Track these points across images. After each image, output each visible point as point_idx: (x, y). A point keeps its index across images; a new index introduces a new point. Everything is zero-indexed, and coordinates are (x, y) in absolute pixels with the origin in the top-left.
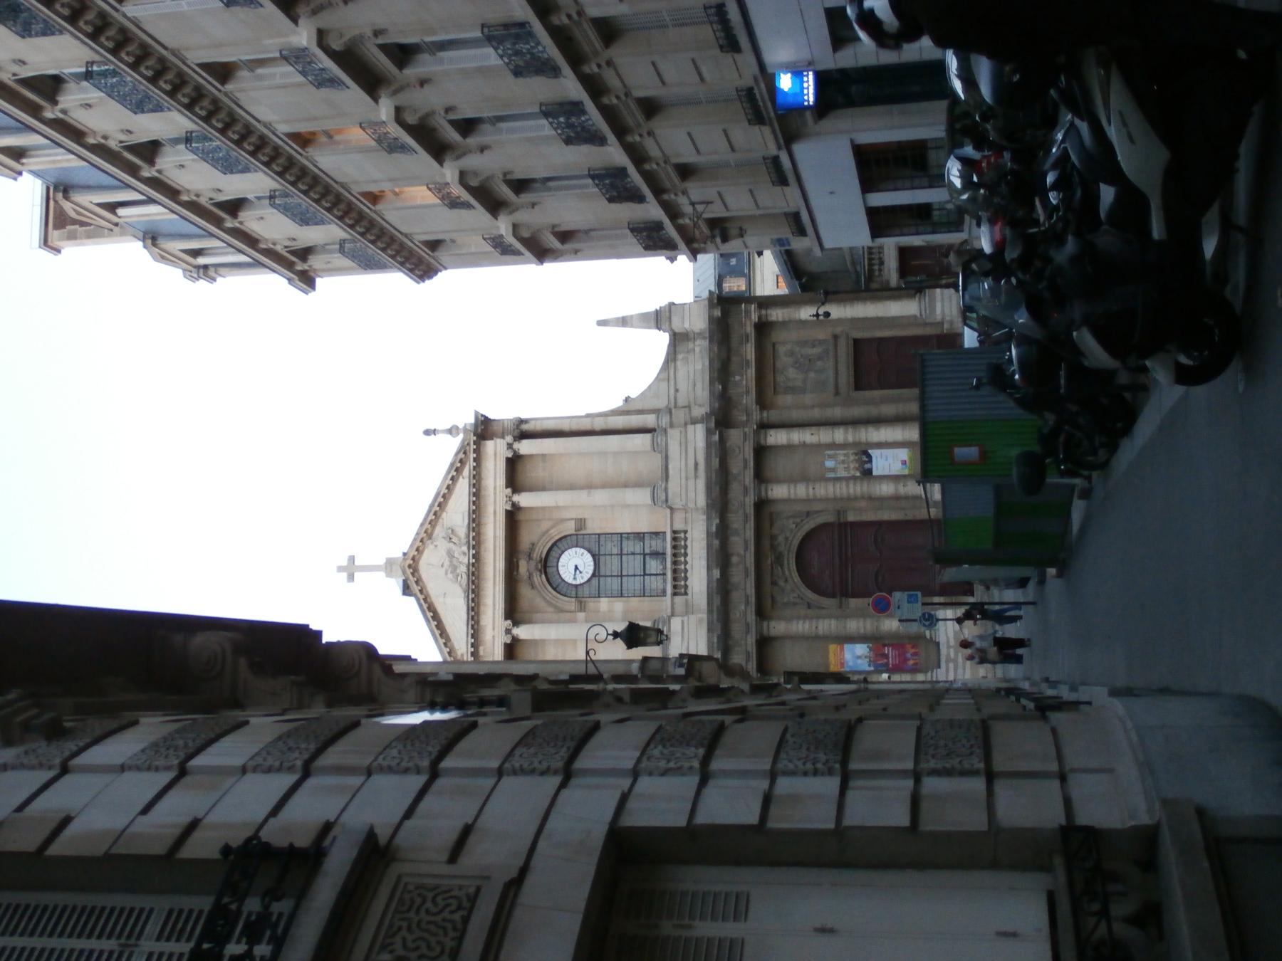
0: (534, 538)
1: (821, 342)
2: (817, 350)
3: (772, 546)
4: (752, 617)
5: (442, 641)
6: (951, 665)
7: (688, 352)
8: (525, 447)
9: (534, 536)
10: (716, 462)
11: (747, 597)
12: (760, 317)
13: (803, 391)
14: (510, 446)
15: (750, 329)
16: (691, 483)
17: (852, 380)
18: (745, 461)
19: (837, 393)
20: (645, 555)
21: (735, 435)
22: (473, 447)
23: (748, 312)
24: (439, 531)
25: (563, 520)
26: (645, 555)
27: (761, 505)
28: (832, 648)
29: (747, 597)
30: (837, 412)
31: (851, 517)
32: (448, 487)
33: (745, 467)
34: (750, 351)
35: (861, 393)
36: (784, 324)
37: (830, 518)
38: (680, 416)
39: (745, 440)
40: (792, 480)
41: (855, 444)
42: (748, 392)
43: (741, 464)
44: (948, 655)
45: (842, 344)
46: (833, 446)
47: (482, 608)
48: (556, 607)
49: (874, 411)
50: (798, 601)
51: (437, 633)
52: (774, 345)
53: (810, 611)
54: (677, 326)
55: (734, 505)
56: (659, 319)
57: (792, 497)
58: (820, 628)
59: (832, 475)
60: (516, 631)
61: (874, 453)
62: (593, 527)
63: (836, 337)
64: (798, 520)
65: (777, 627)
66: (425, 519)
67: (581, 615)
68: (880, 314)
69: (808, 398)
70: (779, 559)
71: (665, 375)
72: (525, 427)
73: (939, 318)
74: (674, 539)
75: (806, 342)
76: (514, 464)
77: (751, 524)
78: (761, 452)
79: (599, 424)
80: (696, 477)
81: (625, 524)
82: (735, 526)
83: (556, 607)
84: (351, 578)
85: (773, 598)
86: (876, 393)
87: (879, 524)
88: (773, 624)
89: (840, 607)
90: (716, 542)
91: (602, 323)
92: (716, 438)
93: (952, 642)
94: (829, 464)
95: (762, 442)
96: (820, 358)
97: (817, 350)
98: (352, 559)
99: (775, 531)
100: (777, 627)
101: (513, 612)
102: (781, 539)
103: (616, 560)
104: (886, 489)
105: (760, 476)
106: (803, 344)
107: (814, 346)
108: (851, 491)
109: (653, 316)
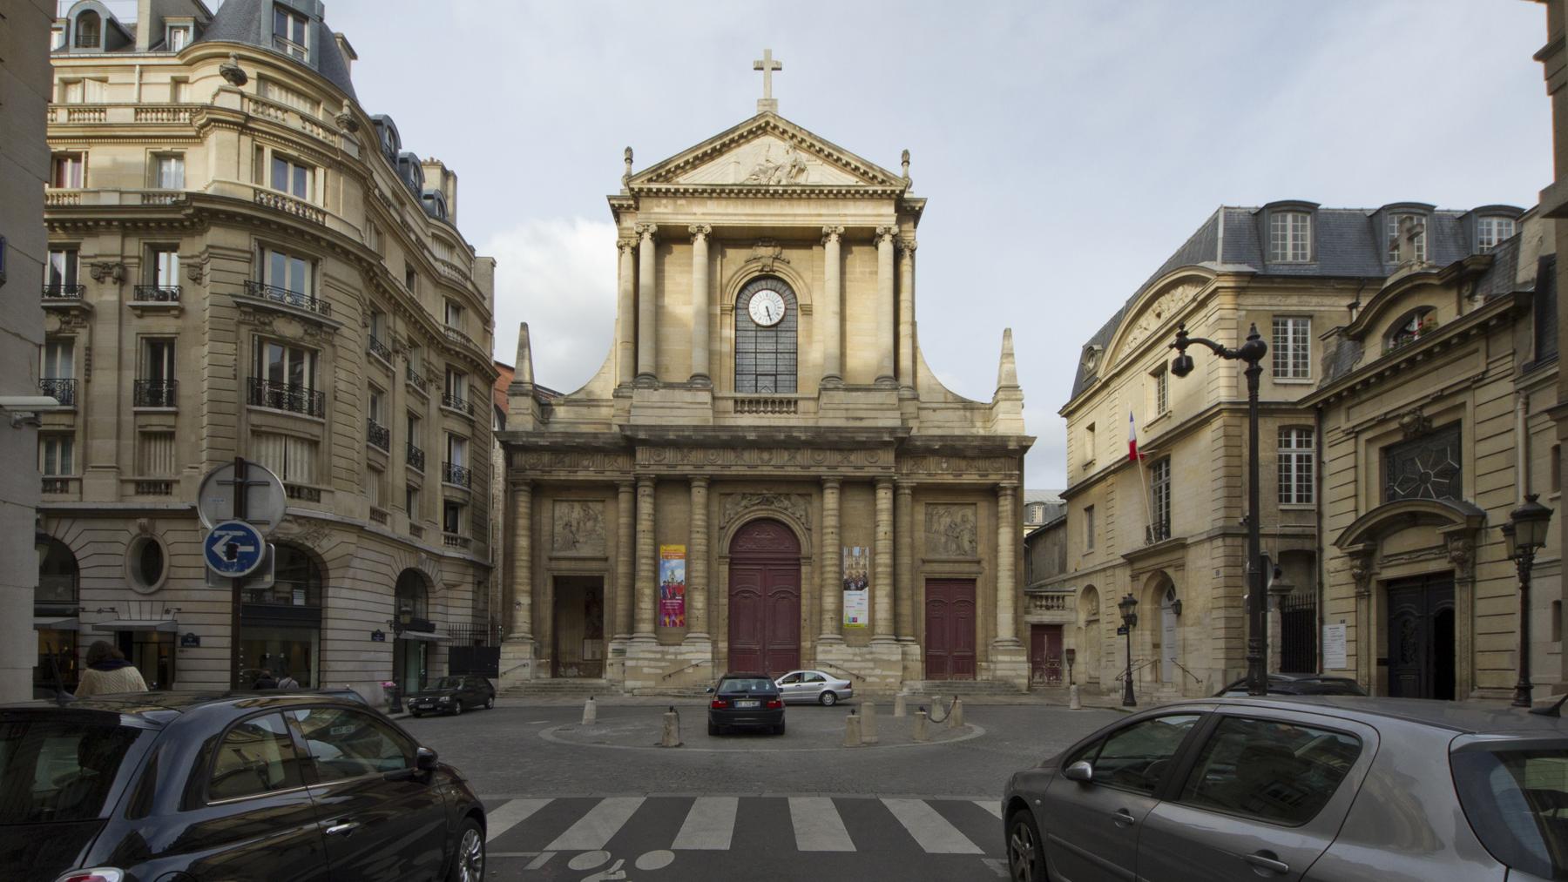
4: (709, 470)
13: (928, 530)
15: (993, 478)
17: (937, 576)
18: (862, 468)
19: (924, 562)
21: (888, 458)
23: (1011, 476)
25: (810, 293)
28: (682, 548)
30: (905, 560)
31: (804, 569)
33: (856, 468)
34: (970, 478)
35: (923, 583)
36: (996, 516)
37: (805, 550)
40: (841, 514)
41: (875, 575)
45: (974, 568)
46: (874, 553)
49: (905, 594)
54: (1002, 406)
55: (819, 456)
59: (845, 552)
61: (865, 593)
63: (979, 562)
65: (699, 494)
69: (920, 535)
70: (768, 501)
74: (789, 402)
77: (799, 472)
78: (870, 485)
82: (799, 456)
86: (922, 598)
87: (799, 597)
88: (703, 491)
90: (782, 436)
94: (856, 551)
96: (959, 547)
100: (699, 494)
103: (772, 347)
104: (829, 601)
105: (847, 485)
106: (974, 531)
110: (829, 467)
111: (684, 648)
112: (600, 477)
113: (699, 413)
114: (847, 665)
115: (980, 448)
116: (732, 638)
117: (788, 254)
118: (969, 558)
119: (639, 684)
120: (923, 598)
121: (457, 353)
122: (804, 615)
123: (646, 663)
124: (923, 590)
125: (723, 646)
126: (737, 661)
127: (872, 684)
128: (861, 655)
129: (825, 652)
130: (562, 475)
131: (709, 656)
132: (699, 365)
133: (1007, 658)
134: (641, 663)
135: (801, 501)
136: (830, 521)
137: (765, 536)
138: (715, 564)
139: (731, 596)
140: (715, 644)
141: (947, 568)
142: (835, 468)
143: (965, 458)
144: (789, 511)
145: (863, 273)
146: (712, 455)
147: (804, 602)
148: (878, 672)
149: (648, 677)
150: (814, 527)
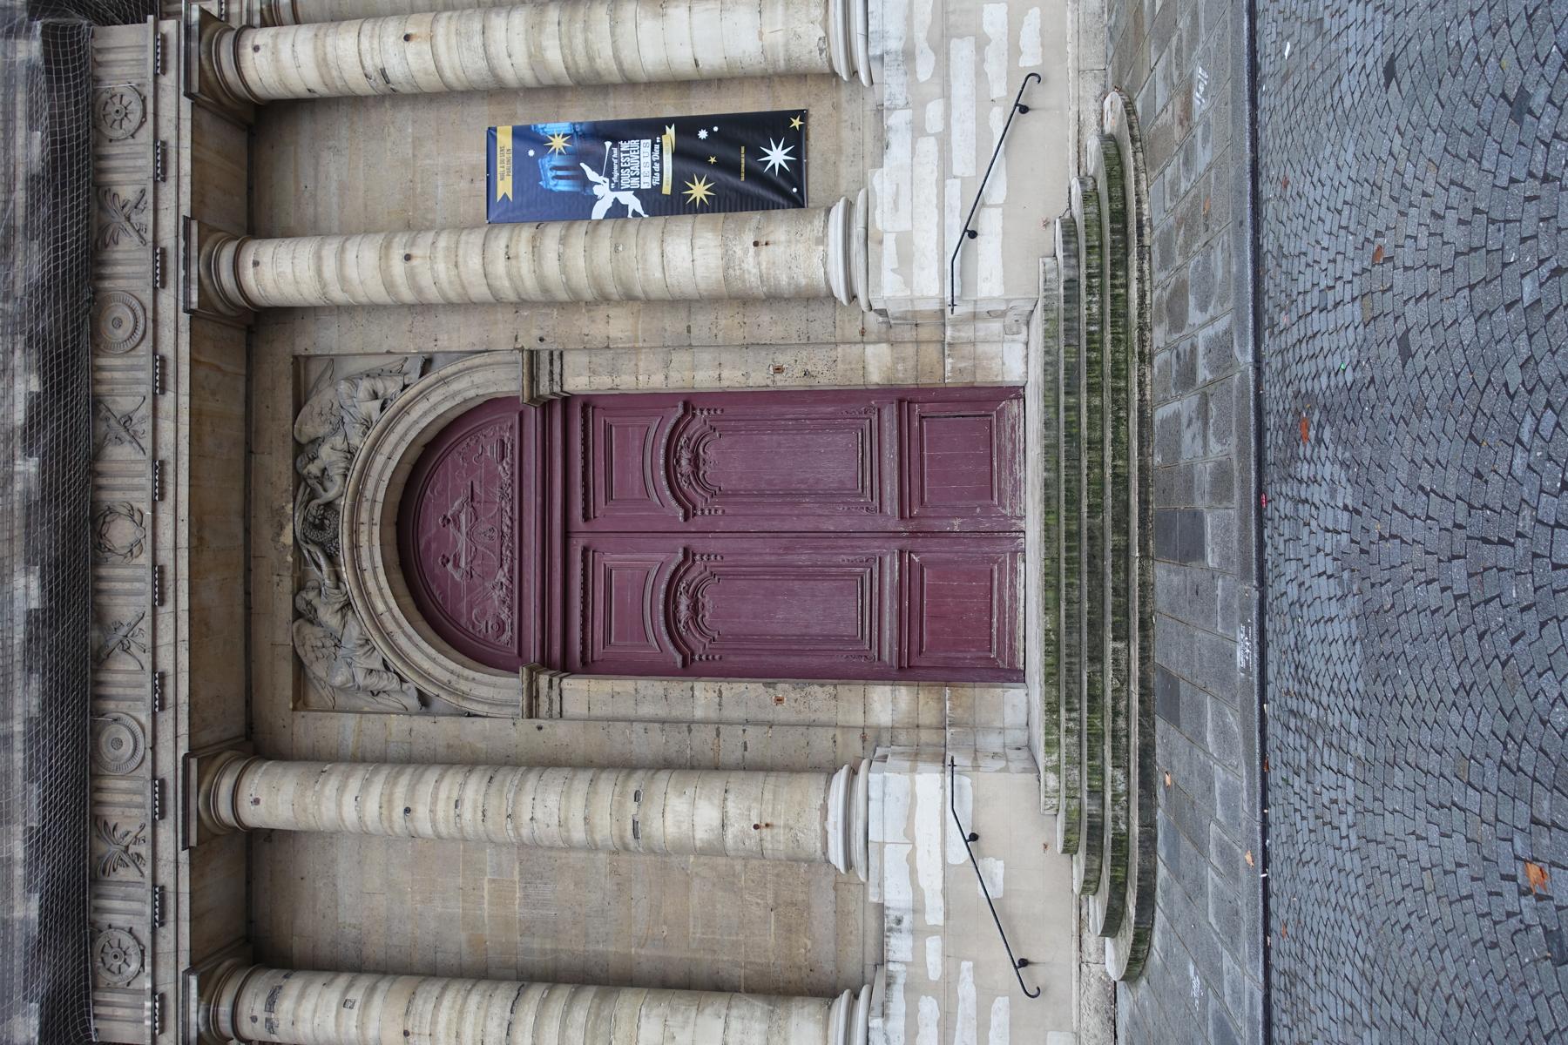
3: (299, 479)
6: (929, 1008)
11: (159, 679)
18: (161, 151)
29: (159, 679)
31: (577, 382)
33: (160, 176)
37: (505, 381)
39: (161, 68)
43: (147, 162)
50: (388, 682)
53: (422, 724)
55: (121, 323)
57: (337, 295)
58: (421, 811)
65: (270, 798)
70: (320, 524)
85: (300, 667)
87: (690, 402)
89: (532, 712)
93: (935, 917)
99: (311, 427)
100: (270, 798)
102: (328, 454)
108: (551, 267)
110: (159, 282)
111: (896, 895)
114: (965, 163)
125: (887, 704)
126: (944, 646)
128: (916, 104)
129: (906, 259)
131: (929, 781)
135: (323, 398)
138: (559, 733)
139: (689, 668)
140: (877, 743)
142: (160, 255)
144: (362, 438)
150: (406, 339)
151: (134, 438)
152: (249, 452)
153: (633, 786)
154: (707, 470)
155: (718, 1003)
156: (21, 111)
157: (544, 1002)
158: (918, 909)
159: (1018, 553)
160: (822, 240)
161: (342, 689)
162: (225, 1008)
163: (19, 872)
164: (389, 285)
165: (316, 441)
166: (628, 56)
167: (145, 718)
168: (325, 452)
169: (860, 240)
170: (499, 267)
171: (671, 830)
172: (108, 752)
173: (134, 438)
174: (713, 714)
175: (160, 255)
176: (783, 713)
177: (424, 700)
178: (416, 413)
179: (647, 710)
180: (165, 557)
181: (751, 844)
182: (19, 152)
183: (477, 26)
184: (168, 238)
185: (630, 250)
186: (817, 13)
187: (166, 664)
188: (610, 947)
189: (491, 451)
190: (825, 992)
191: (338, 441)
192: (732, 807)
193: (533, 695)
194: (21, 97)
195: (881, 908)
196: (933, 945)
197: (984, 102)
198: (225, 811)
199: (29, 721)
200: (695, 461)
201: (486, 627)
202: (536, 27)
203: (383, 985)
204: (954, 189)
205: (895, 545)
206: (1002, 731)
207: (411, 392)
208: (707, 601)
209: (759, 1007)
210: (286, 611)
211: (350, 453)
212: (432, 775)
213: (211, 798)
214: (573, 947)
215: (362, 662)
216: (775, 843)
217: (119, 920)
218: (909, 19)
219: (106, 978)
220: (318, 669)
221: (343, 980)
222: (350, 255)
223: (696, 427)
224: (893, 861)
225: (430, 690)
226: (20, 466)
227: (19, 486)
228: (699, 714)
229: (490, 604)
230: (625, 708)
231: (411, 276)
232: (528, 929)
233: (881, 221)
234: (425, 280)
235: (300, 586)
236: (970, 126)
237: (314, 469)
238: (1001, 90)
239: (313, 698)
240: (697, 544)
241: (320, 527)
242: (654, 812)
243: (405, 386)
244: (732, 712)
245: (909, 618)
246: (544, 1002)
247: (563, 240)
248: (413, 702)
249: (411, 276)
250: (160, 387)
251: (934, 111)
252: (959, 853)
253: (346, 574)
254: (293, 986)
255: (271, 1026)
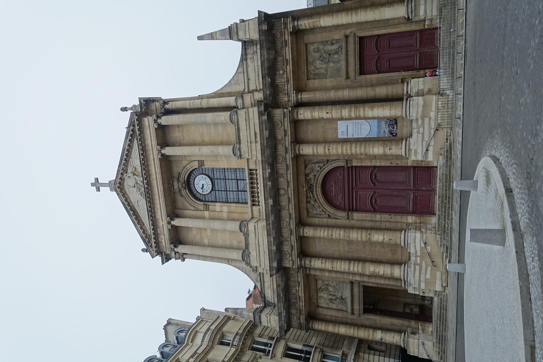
0: (180, 170)
1: (338, 41)
2: (335, 47)
3: (306, 180)
4: (293, 226)
5: (139, 226)
6: (417, 267)
7: (253, 54)
8: (165, 120)
9: (181, 169)
10: (266, 133)
11: (290, 215)
12: (294, 27)
14: (156, 121)
15: (288, 37)
16: (253, 145)
17: (358, 67)
19: (348, 77)
20: (237, 180)
21: (278, 113)
22: (136, 123)
23: (285, 24)
24: (130, 170)
26: (237, 180)
27: (297, 157)
29: (290, 215)
30: (346, 94)
31: (355, 164)
32: (129, 145)
33: (285, 135)
34: (288, 53)
35: (363, 77)
36: (312, 30)
38: (248, 99)
39: (284, 117)
40: (316, 142)
42: (288, 81)
44: (416, 260)
45: (351, 40)
47: (156, 209)
48: (194, 207)
49: (370, 93)
51: (136, 222)
52: (306, 44)
53: (329, 220)
54: (241, 36)
55: (280, 159)
56: (231, 33)
58: (334, 235)
60: (173, 223)
62: (208, 165)
63: (347, 37)
64: (322, 165)
65: (309, 232)
66: (120, 163)
67: (207, 213)
68: (377, 18)
69: (329, 82)
70: (310, 188)
71: (241, 70)
72: (167, 106)
73: (422, 18)
74: (251, 174)
75: (327, 42)
76: (162, 131)
77: (290, 171)
78: (296, 123)
79: (205, 103)
80: (256, 142)
81: (223, 164)
82: (281, 172)
83: (194, 207)
84: (98, 190)
89: (348, 219)
91: (200, 38)
92: (265, 117)
93: (419, 254)
95: (296, 118)
96: (336, 53)
97: (335, 47)
98: (97, 179)
99: (308, 171)
101: (173, 213)
103: (223, 182)
107: (332, 44)
108: (353, 151)
109: (228, 33)
110: (286, 152)
111: (412, 251)
112: (302, 284)
113: (260, 230)
114: (426, 138)
115: (269, 49)
116: (405, 212)
117: (176, 174)
118: (344, 45)
119: (438, 282)
120: (375, 76)
121: (243, 344)
122: (388, 164)
123: (423, 276)
124: (368, 76)
125: (411, 219)
127: (443, 119)
128: (418, 128)
130: (302, 304)
132: (235, 226)
133: (422, 8)
134: (423, 279)
135: (310, 166)
136: (321, 150)
137: (333, 189)
138: (353, 222)
139: (375, 211)
141: (351, 60)
142: (286, 149)
143: (275, 59)
145: (179, 132)
146: (284, 224)
147: (378, 164)
148: (432, 114)
149: (433, 275)
151: (283, 177)
152: (297, 176)
153: (368, 233)
154: (378, 178)
155: (383, 265)
156: (264, 128)
157: (354, 264)
158: (416, 253)
159: (435, 194)
160: (401, 149)
161: (315, 214)
162: (303, 263)
163: (272, 243)
164: (325, 153)
165: (309, 174)
166: (366, 116)
167: (288, 220)
168: (311, 176)
169: (408, 150)
170: (345, 151)
171: (375, 240)
172: (282, 225)
173: (283, 177)
174: (380, 220)
175: (286, 149)
176: (392, 220)
177: (329, 216)
178: (326, 169)
179: (368, 219)
180: (290, 196)
181: (388, 242)
182: (264, 134)
183: (340, 111)
184: (287, 146)
185: (367, 150)
186: (401, 110)
187: (291, 212)
188: (362, 255)
189: (338, 174)
190: (400, 264)
191: (313, 174)
192: (385, 237)
193: (348, 216)
194: (264, 125)
195: (410, 253)
196: (418, 259)
197: (430, 128)
198: (301, 234)
199: (272, 221)
200: (376, 176)
201: (338, 203)
202: (350, 111)
203: (327, 260)
204: (424, 143)
205: (412, 192)
206: (431, 224)
207: (325, 166)
208: (378, 200)
209: (389, 266)
210: (305, 201)
211: (315, 176)
212: (335, 230)
213: (299, 232)
214: (356, 255)
215: (319, 210)
216: (392, 242)
217: (285, 249)
218: (417, 114)
219: (284, 257)
220: (311, 211)
221: (321, 259)
222: (319, 149)
223: (376, 171)
224: (412, 246)
225: (331, 215)
226: (268, 183)
227: (268, 187)
228: (377, 219)
229: (339, 200)
230: (364, 218)
231: (329, 152)
232: (348, 252)
233: (412, 147)
234: (332, 153)
235: (307, 198)
236: (428, 132)
237: (309, 178)
238: (433, 126)
239: (310, 215)
240: (376, 190)
241: (310, 188)
242: (372, 237)
243: (324, 165)
244: (383, 219)
245: (415, 204)
246: (354, 264)
247: (356, 147)
248: (327, 216)
249: (329, 152)
250: (287, 169)
251: (421, 129)
252: (423, 245)
253: (315, 196)
254: (313, 260)
255: (310, 265)
